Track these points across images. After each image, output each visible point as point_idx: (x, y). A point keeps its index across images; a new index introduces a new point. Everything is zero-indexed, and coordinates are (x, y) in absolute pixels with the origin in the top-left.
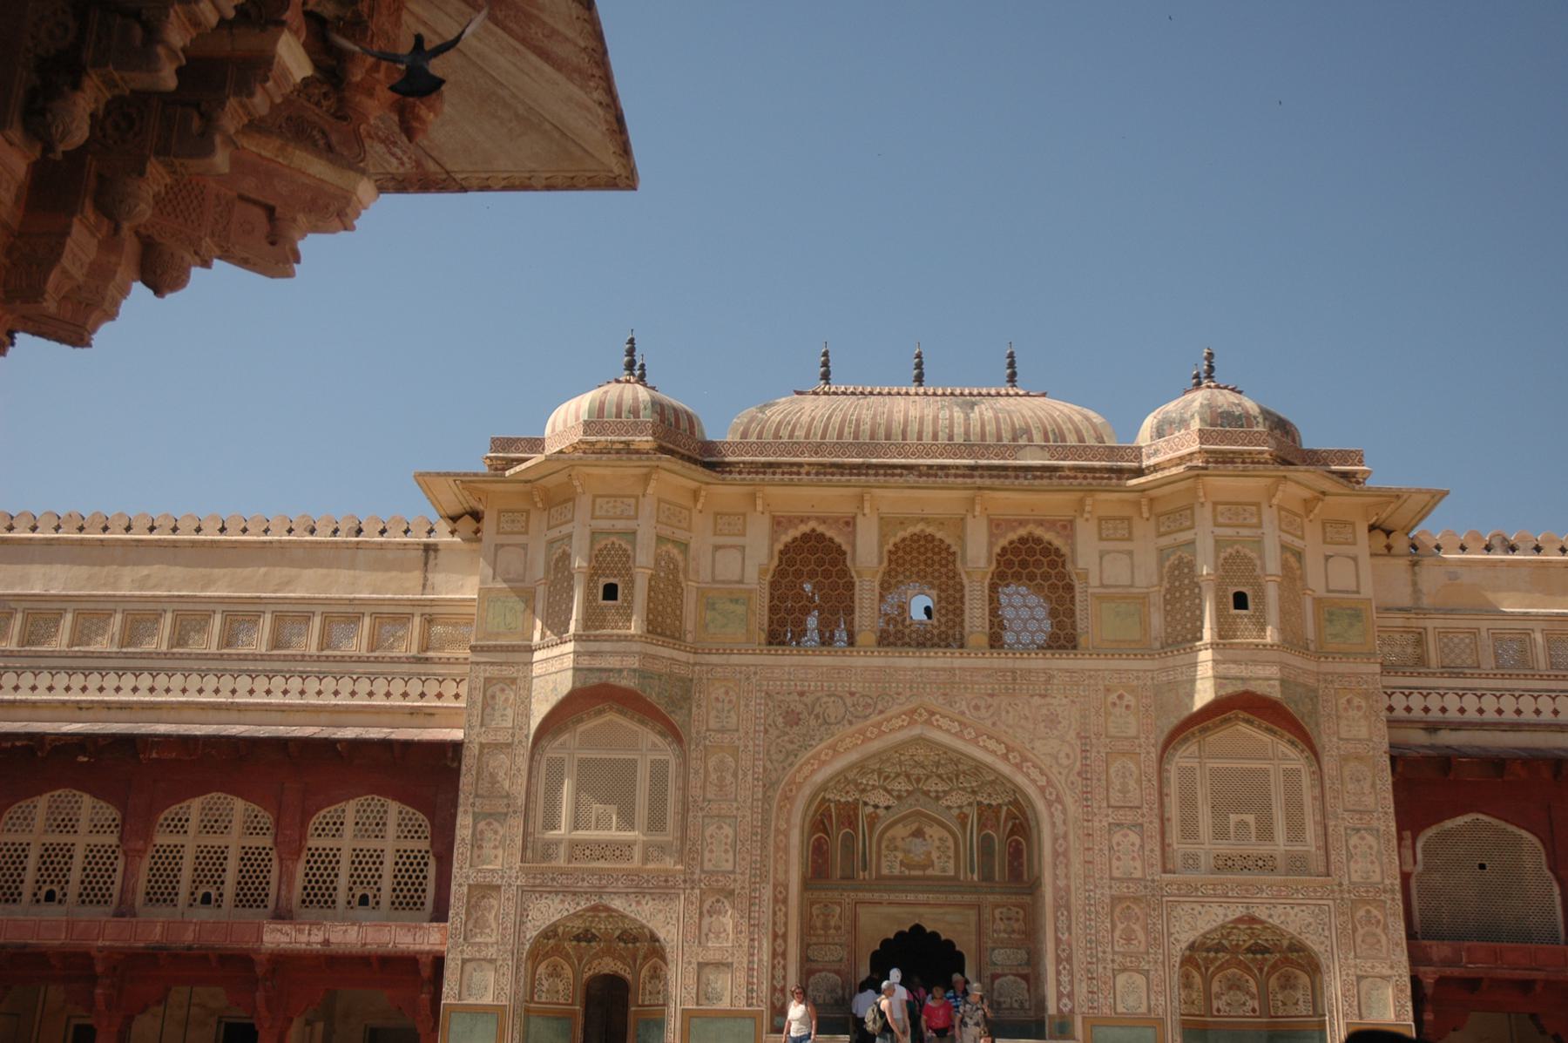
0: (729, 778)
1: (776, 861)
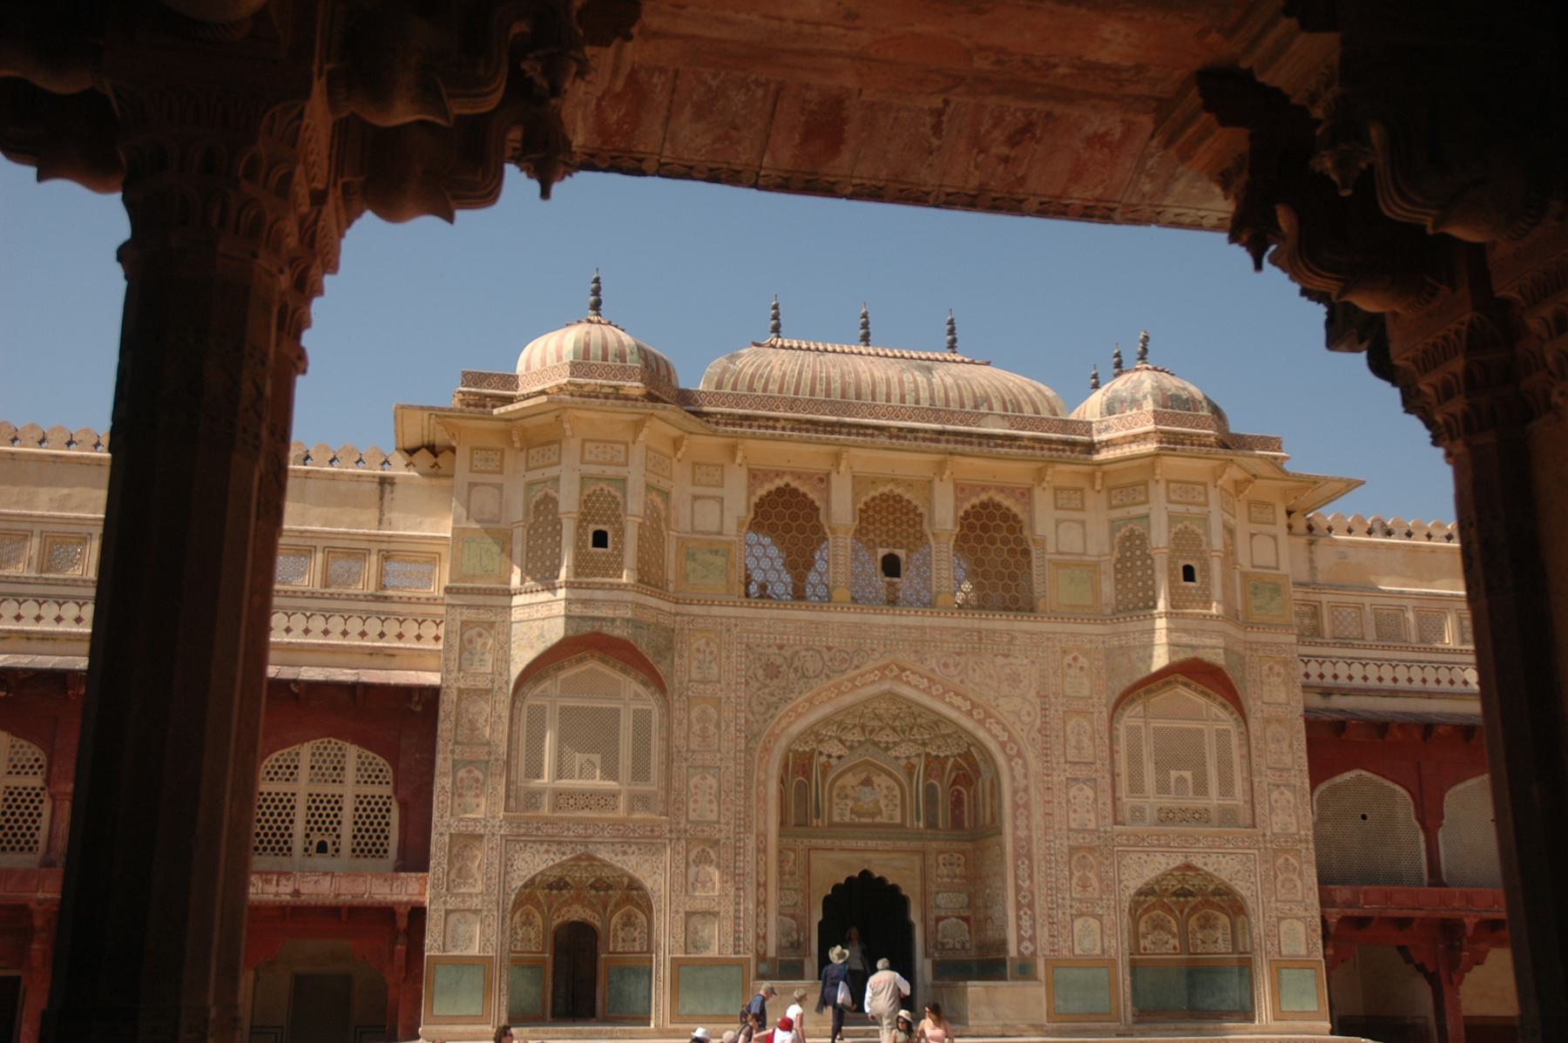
0: (712, 729)
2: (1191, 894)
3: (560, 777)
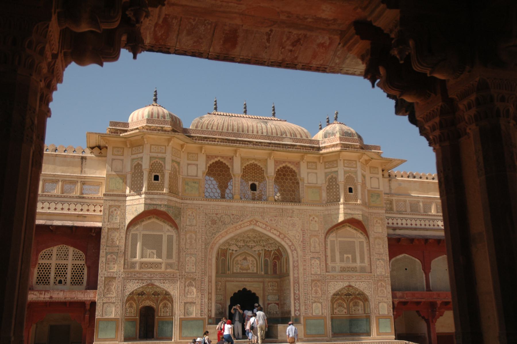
0: (194, 241)
2: (351, 295)
3: (142, 257)
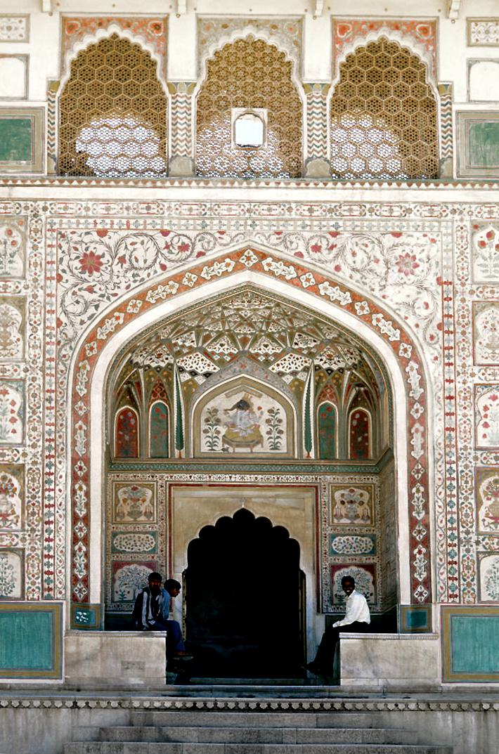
1: (74, 432)
